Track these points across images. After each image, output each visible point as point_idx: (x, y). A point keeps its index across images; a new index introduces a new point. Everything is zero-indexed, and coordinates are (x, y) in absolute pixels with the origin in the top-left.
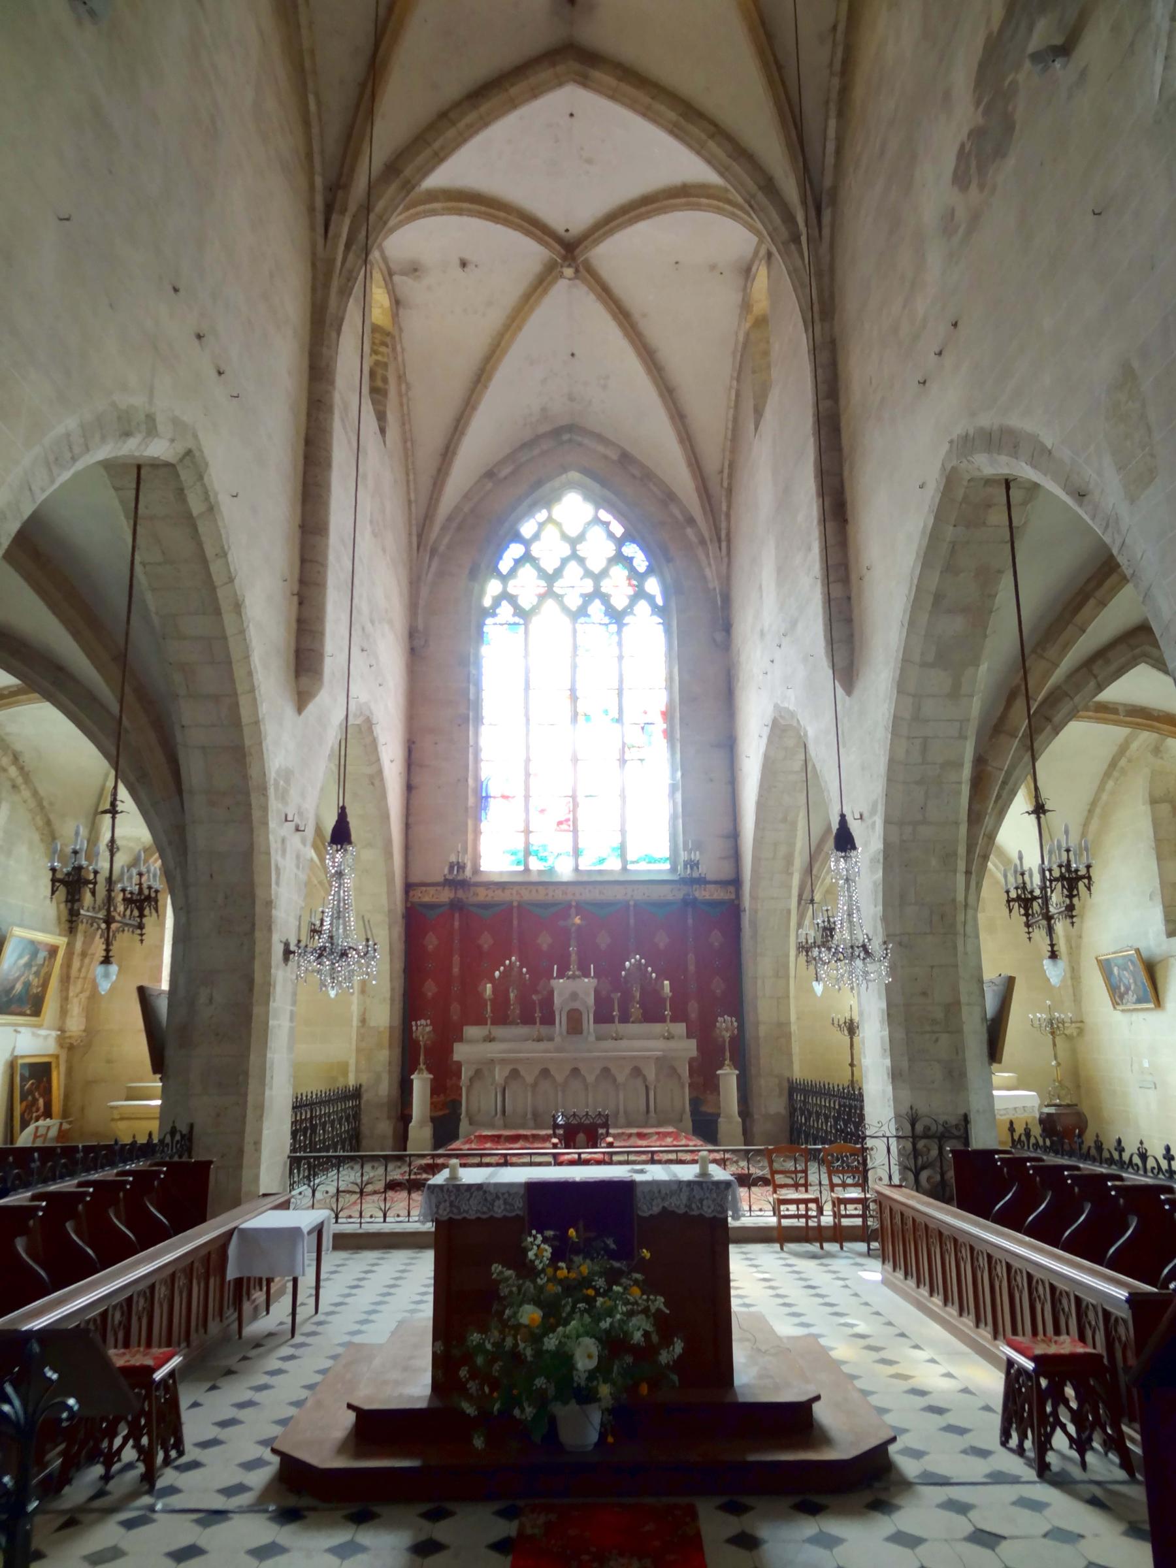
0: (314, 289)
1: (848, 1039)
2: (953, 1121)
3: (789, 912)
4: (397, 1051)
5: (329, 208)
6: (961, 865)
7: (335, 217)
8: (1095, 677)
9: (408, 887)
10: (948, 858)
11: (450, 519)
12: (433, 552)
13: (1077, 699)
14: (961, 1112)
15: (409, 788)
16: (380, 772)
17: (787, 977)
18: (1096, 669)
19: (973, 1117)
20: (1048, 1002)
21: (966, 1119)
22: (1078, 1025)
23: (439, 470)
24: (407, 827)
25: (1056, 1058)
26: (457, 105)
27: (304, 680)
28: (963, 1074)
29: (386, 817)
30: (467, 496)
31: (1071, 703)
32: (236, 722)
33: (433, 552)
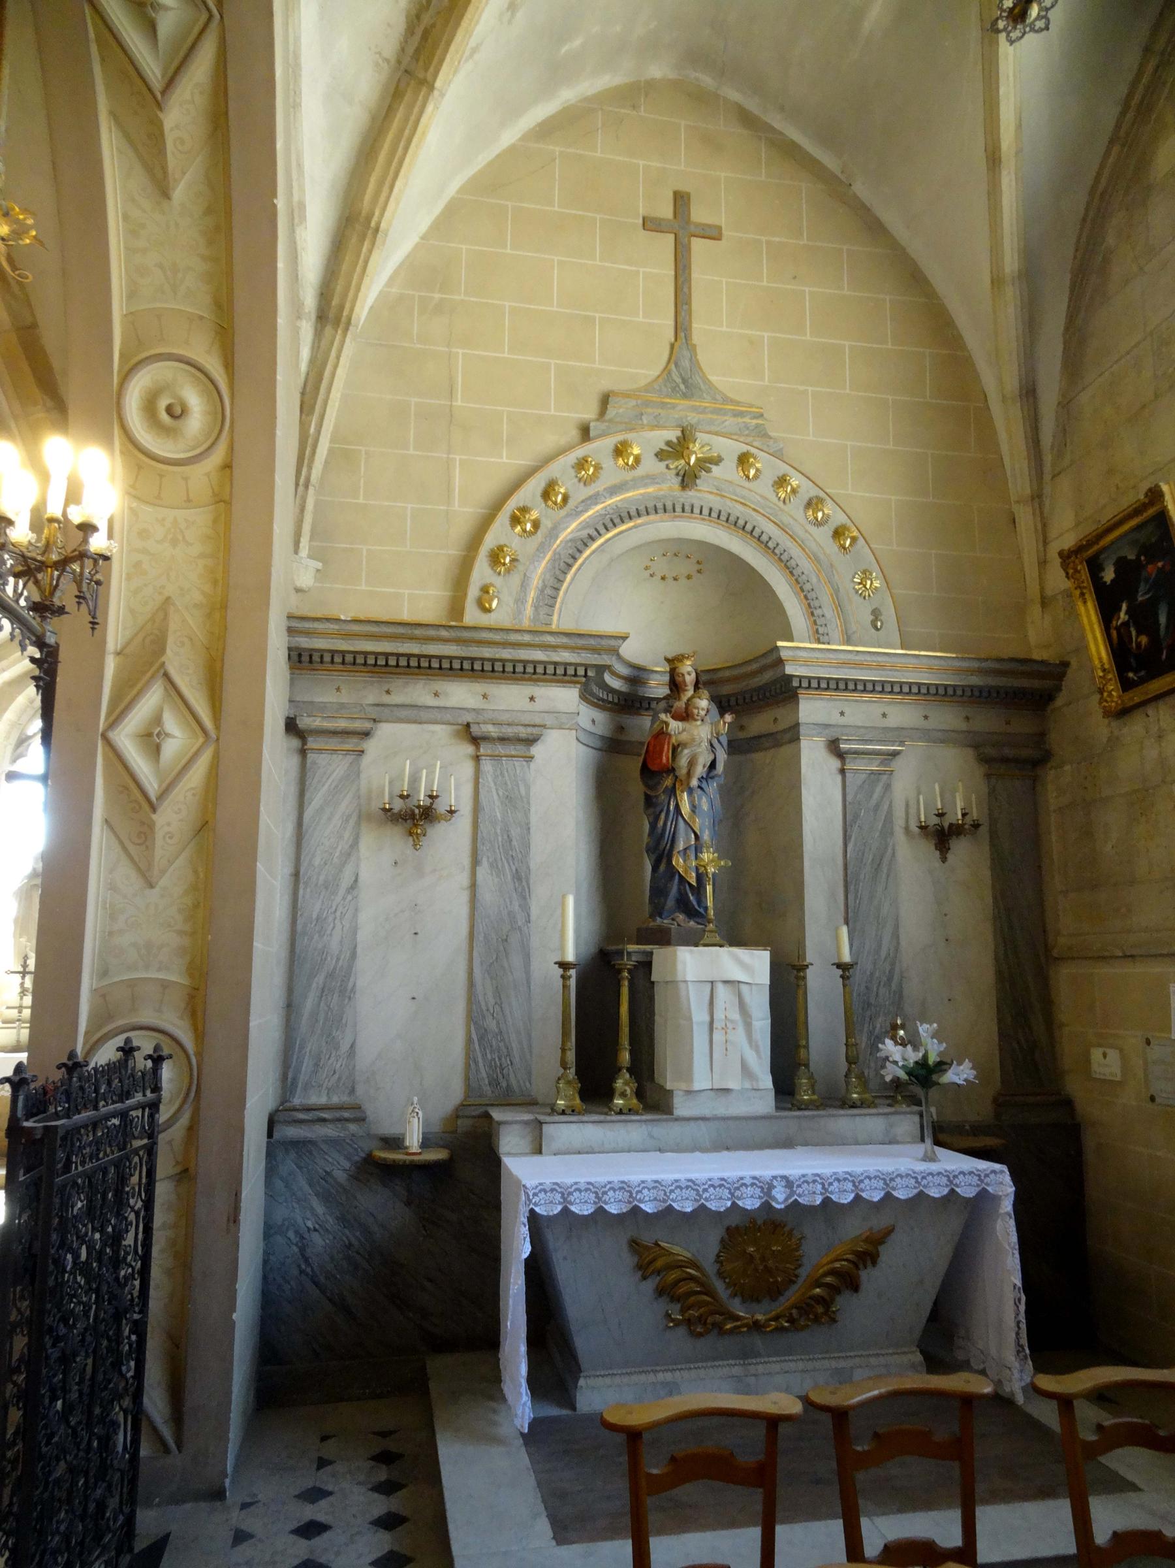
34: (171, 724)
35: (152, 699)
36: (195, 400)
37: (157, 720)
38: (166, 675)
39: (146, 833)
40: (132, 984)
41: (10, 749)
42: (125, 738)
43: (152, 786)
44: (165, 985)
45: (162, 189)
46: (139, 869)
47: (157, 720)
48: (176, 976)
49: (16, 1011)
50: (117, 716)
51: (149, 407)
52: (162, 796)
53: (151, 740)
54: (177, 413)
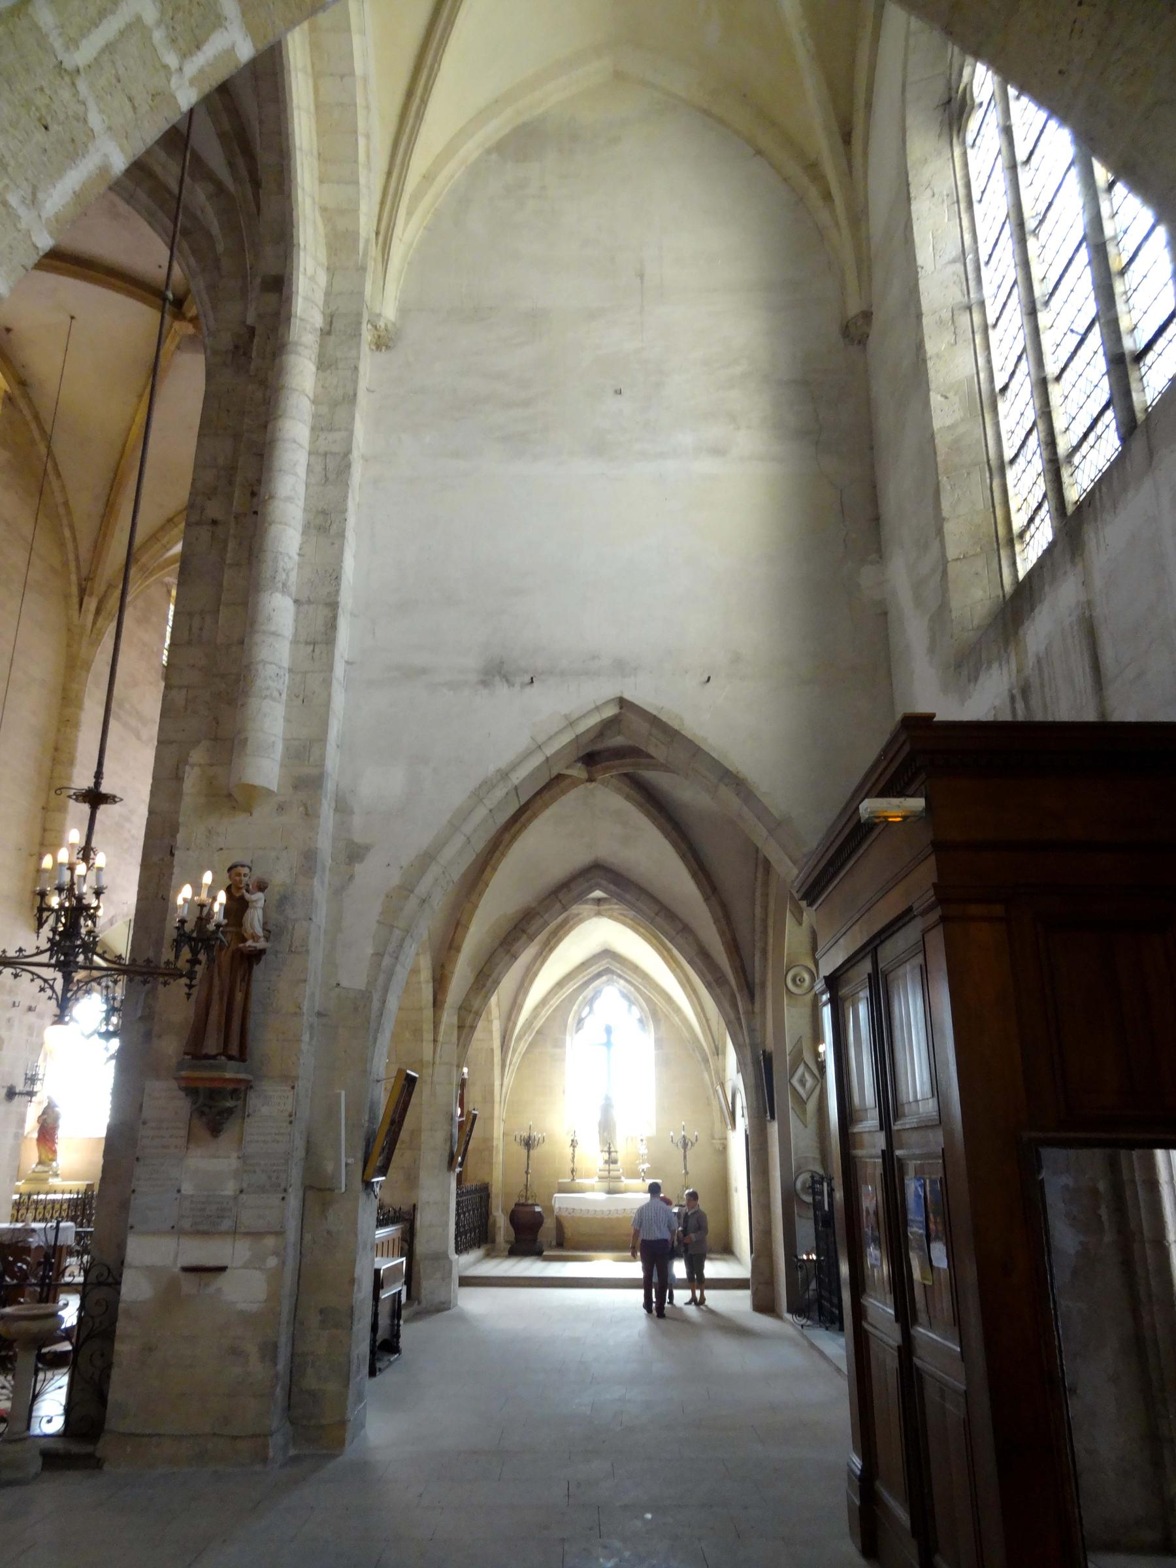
1: (526, 1151)
2: (405, 1208)
3: (492, 1050)
6: (428, 1036)
7: (86, 599)
8: (560, 901)
10: (417, 1032)
13: (546, 916)
14: (412, 1202)
17: (493, 1102)
18: (560, 896)
19: (419, 1206)
20: (683, 1123)
21: (414, 1206)
22: (722, 1141)
25: (685, 1168)
28: (417, 1177)
31: (542, 919)
34: (808, 1077)
35: (801, 1069)
36: (807, 977)
37: (803, 1075)
38: (805, 1062)
39: (804, 1111)
40: (806, 1157)
41: (575, 1025)
42: (795, 1081)
43: (804, 1096)
44: (814, 1158)
45: (800, 923)
46: (803, 1124)
47: (803, 1075)
48: (818, 1156)
49: (607, 1173)
50: (792, 1076)
51: (794, 980)
52: (808, 1099)
53: (802, 1082)
54: (802, 980)
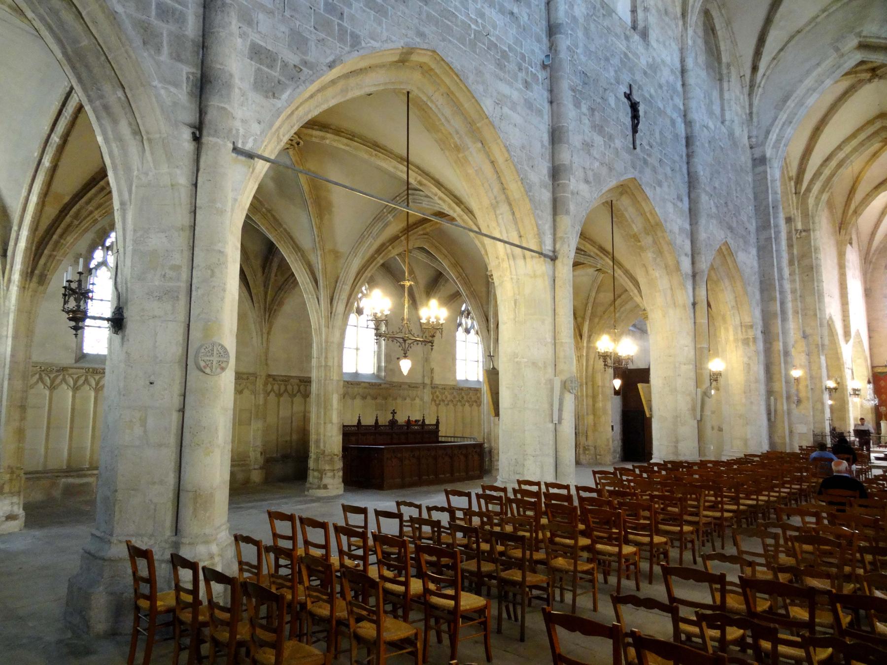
0: (838, 249)
4: (874, 415)
5: (840, 229)
9: (873, 367)
11: (875, 251)
12: (871, 262)
15: (870, 337)
16: (862, 341)
23: (870, 239)
24: (870, 349)
26: (871, 191)
27: (847, 338)
29: (864, 351)
30: (881, 243)
32: (837, 353)
33: (871, 262)
